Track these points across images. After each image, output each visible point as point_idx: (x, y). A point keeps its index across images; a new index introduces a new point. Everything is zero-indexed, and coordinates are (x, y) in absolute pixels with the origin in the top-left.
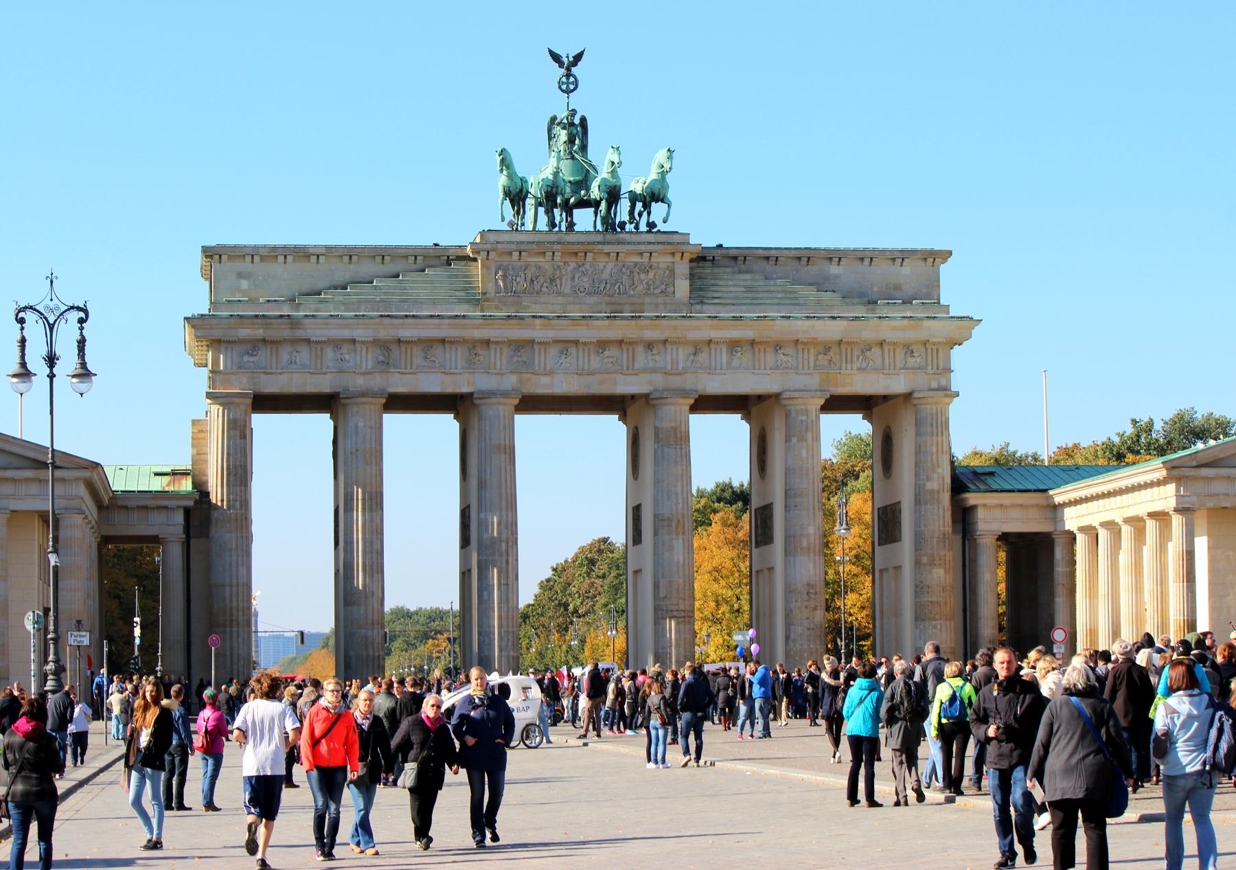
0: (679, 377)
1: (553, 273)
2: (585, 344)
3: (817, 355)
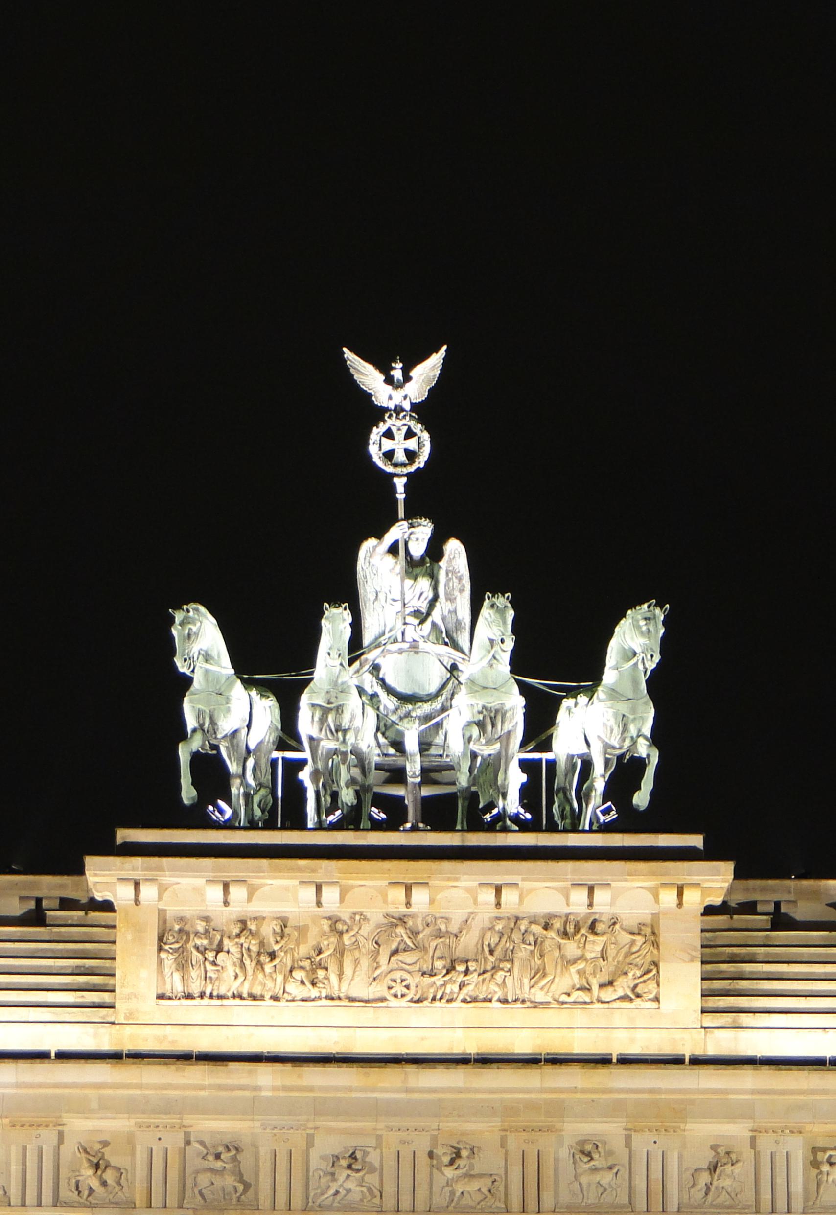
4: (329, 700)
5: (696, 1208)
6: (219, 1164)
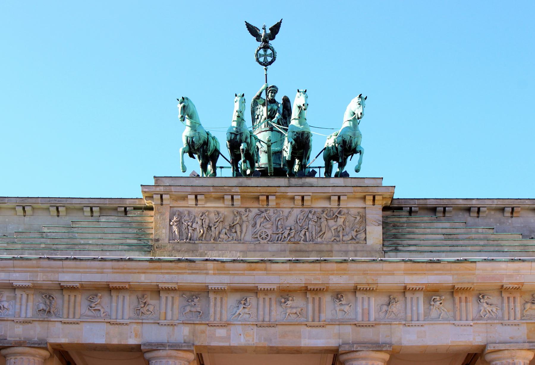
0: (370, 329)
1: (234, 220)
2: (266, 292)
3: (524, 304)
4: (237, 131)
5: (382, 319)
6: (193, 303)
